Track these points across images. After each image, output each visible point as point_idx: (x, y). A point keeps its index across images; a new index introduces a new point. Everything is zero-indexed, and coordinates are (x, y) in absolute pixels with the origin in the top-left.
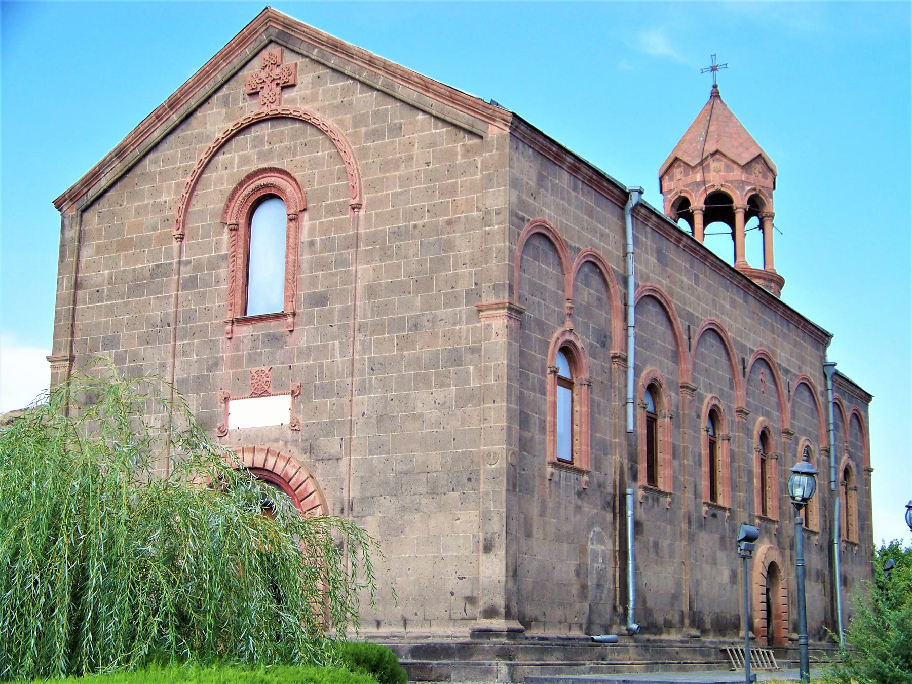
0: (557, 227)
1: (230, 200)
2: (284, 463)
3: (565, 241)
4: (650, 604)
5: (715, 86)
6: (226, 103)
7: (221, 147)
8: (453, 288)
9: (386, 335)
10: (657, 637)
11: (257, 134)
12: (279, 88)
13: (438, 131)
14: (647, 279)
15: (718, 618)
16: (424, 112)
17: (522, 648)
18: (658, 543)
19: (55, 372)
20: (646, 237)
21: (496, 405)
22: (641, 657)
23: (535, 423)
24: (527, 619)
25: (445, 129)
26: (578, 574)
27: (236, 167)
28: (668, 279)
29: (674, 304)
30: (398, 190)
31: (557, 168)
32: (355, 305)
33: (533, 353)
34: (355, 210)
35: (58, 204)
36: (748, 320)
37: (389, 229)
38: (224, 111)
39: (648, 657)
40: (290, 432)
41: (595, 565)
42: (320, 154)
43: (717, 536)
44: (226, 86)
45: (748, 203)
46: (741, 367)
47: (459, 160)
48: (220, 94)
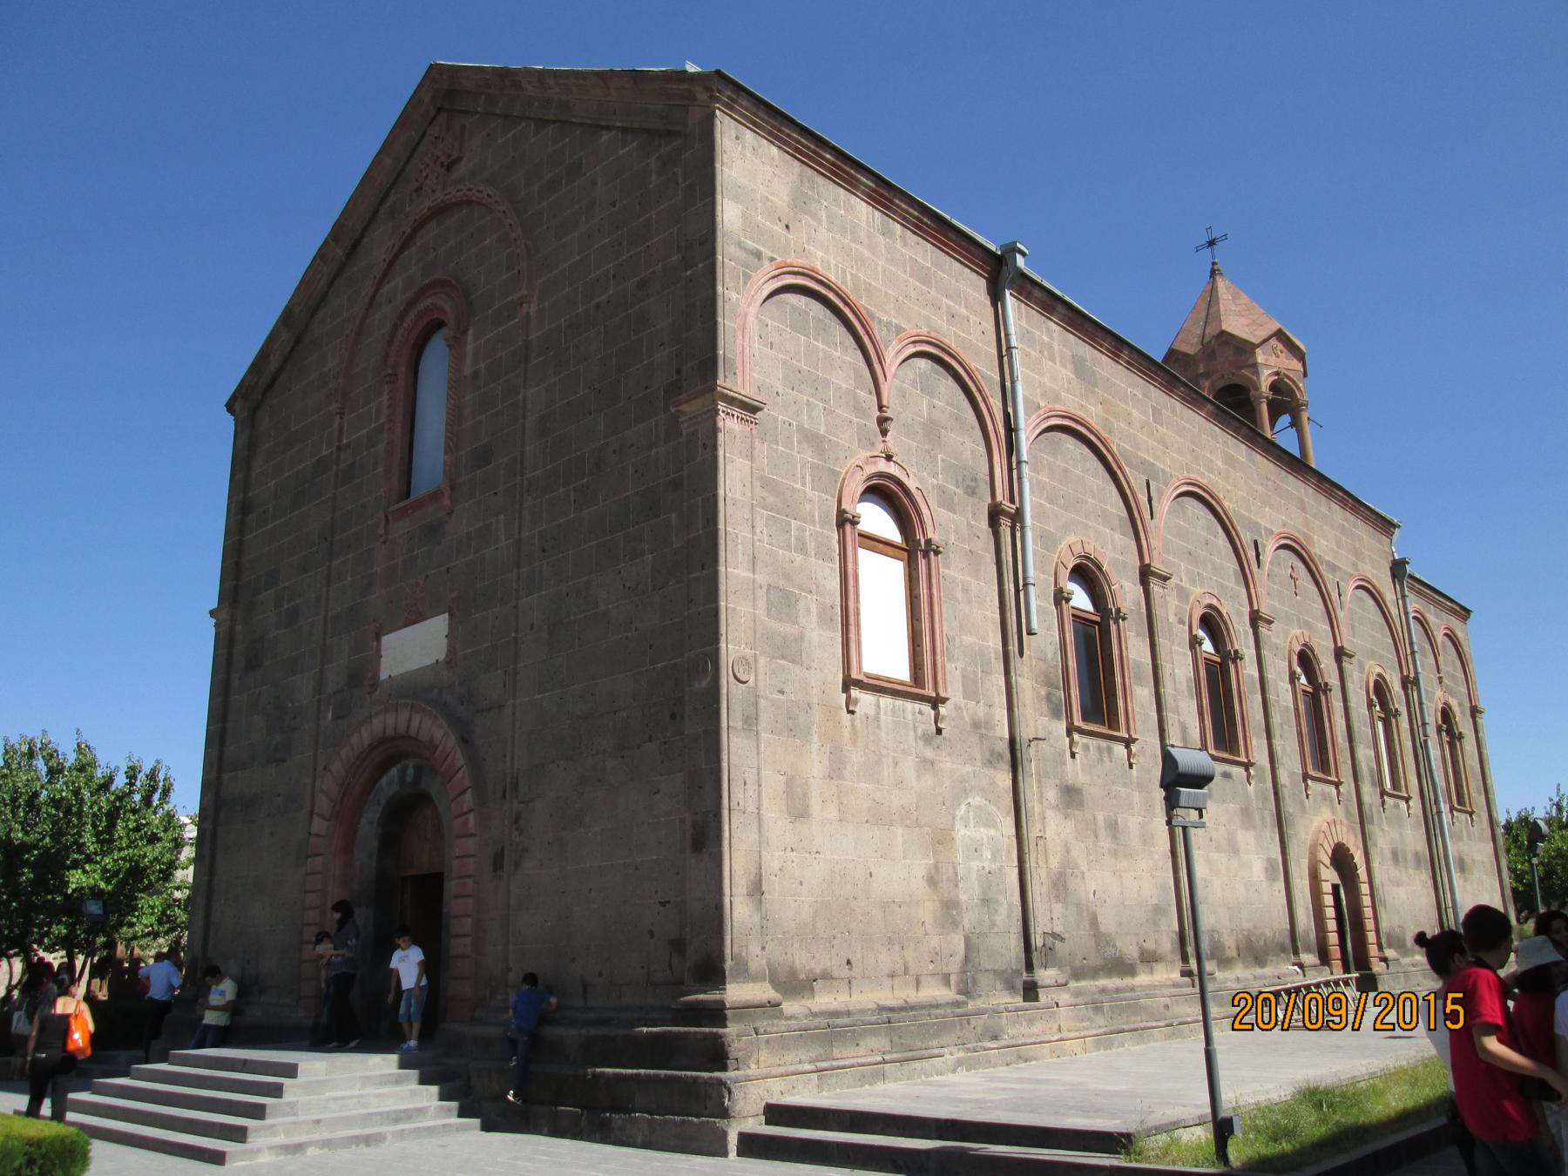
0: (844, 282)
1: (390, 343)
3: (866, 309)
4: (1107, 923)
5: (1214, 264)
7: (386, 274)
8: (647, 388)
9: (561, 490)
10: (1128, 981)
12: (443, 170)
14: (1057, 399)
15: (1249, 935)
16: (608, 128)
17: (767, 1042)
18: (1117, 824)
20: (1052, 338)
21: (705, 572)
22: (1085, 1024)
23: (808, 610)
24: (802, 976)
25: (635, 144)
26: (932, 881)
28: (1100, 406)
29: (1118, 445)
31: (842, 190)
32: (522, 453)
33: (798, 486)
34: (524, 305)
36: (1260, 488)
37: (565, 321)
39: (1101, 1021)
41: (975, 865)
43: (1234, 807)
44: (393, 191)
45: (1270, 390)
46: (1251, 553)
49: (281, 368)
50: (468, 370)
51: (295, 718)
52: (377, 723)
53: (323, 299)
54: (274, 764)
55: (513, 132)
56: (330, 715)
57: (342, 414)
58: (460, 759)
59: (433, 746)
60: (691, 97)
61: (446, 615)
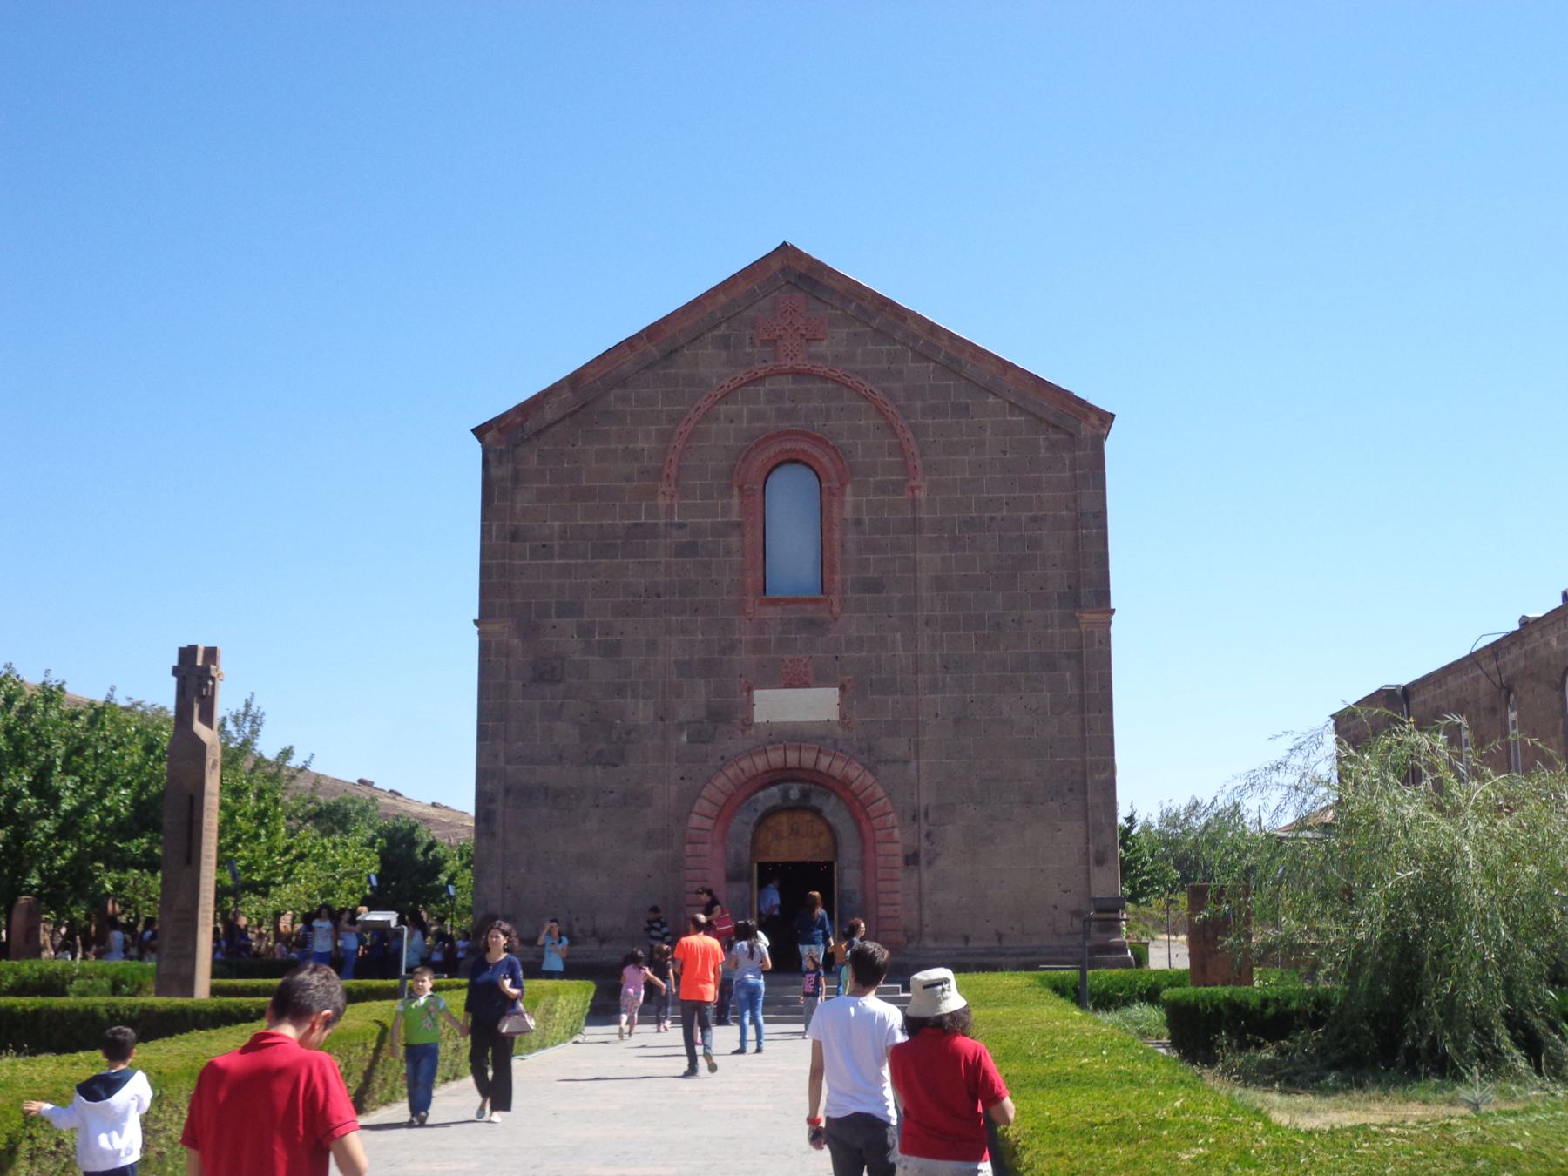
2: (843, 764)
6: (725, 342)
7: (726, 397)
9: (962, 632)
11: (772, 387)
12: (804, 340)
13: (1014, 419)
16: (995, 394)
19: (486, 639)
27: (745, 421)
30: (967, 476)
35: (479, 432)
38: (724, 354)
40: (839, 731)
42: (862, 422)
44: (724, 325)
47: (1043, 454)
48: (716, 332)
49: (557, 422)
50: (848, 513)
51: (628, 733)
52: (776, 757)
53: (623, 382)
54: (597, 766)
55: (888, 347)
56: (684, 738)
57: (673, 496)
58: (880, 792)
59: (845, 783)
60: (1086, 417)
61: (837, 689)
